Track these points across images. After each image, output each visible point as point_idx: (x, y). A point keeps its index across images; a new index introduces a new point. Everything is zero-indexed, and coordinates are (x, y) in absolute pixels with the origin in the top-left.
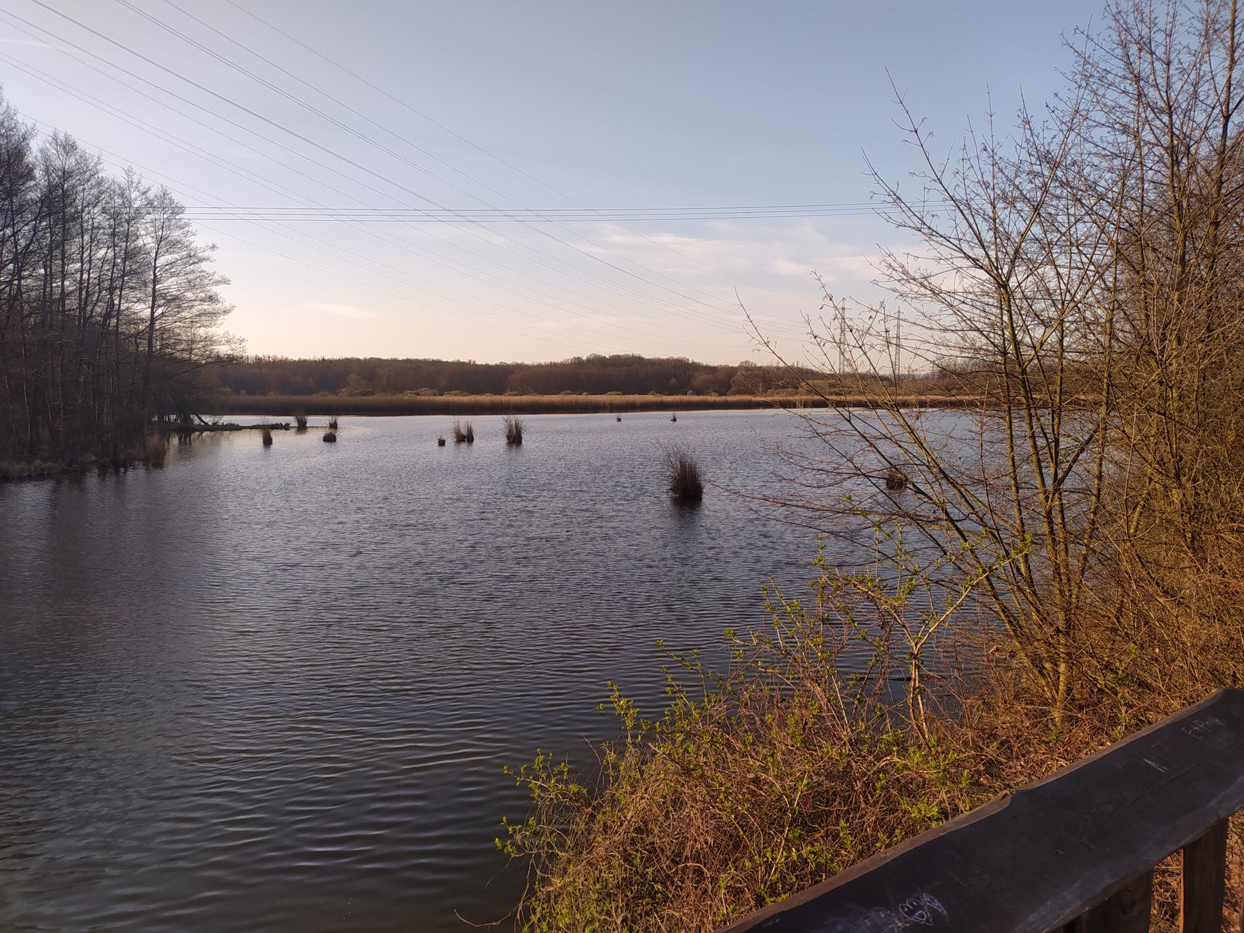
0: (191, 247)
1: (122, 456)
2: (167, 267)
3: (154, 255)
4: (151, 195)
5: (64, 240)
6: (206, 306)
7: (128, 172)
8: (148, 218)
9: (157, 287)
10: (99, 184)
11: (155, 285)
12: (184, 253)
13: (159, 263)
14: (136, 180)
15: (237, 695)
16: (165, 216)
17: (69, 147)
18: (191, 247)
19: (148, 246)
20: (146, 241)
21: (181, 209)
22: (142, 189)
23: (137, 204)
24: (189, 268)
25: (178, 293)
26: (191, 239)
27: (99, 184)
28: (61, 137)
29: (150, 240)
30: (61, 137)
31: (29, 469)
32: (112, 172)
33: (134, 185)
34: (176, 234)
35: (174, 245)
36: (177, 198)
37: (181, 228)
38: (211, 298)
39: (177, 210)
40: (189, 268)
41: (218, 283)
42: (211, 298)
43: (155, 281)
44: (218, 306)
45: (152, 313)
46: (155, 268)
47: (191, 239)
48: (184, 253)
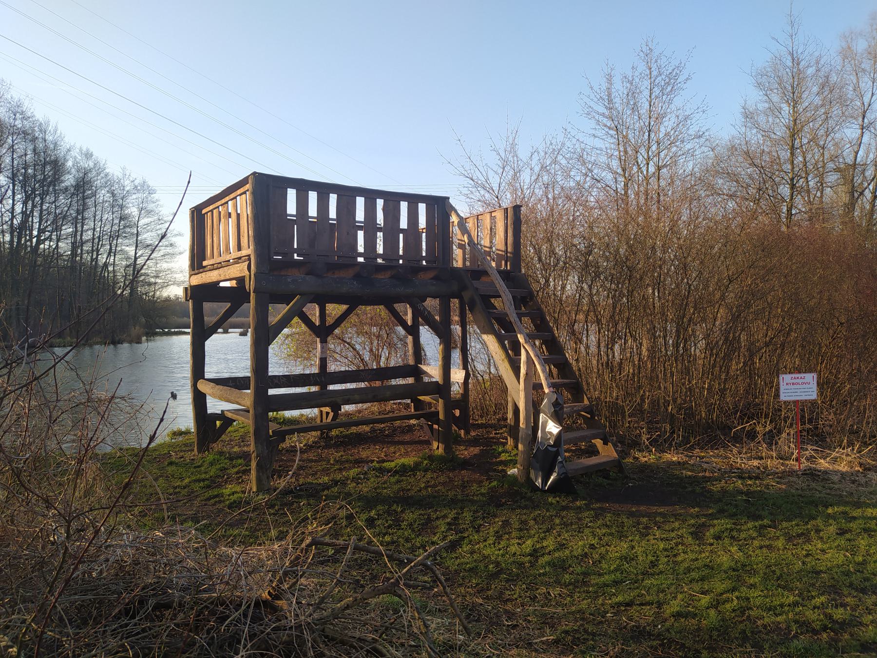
0: (160, 214)
1: (117, 339)
2: (145, 226)
3: (137, 219)
4: (136, 183)
5: (84, 210)
6: (169, 250)
7: (124, 169)
8: (134, 196)
9: (139, 238)
10: (106, 175)
11: (137, 237)
12: (155, 218)
13: (141, 223)
14: (128, 174)
15: (400, 381)
16: (145, 195)
17: (88, 155)
18: (160, 214)
19: (133, 214)
20: (133, 210)
21: (154, 192)
22: (131, 179)
23: (127, 188)
24: (158, 227)
25: (151, 242)
26: (160, 209)
27: (106, 175)
28: (84, 149)
29: (136, 210)
30: (84, 149)
31: (64, 342)
32: (113, 169)
33: (127, 176)
34: (151, 206)
35: (149, 212)
36: (151, 183)
37: (154, 202)
38: (171, 245)
39: (151, 192)
40: (158, 227)
41: (176, 235)
42: (171, 245)
43: (137, 235)
44: (176, 250)
45: (136, 254)
46: (138, 227)
47: (160, 209)
48: (155, 218)
